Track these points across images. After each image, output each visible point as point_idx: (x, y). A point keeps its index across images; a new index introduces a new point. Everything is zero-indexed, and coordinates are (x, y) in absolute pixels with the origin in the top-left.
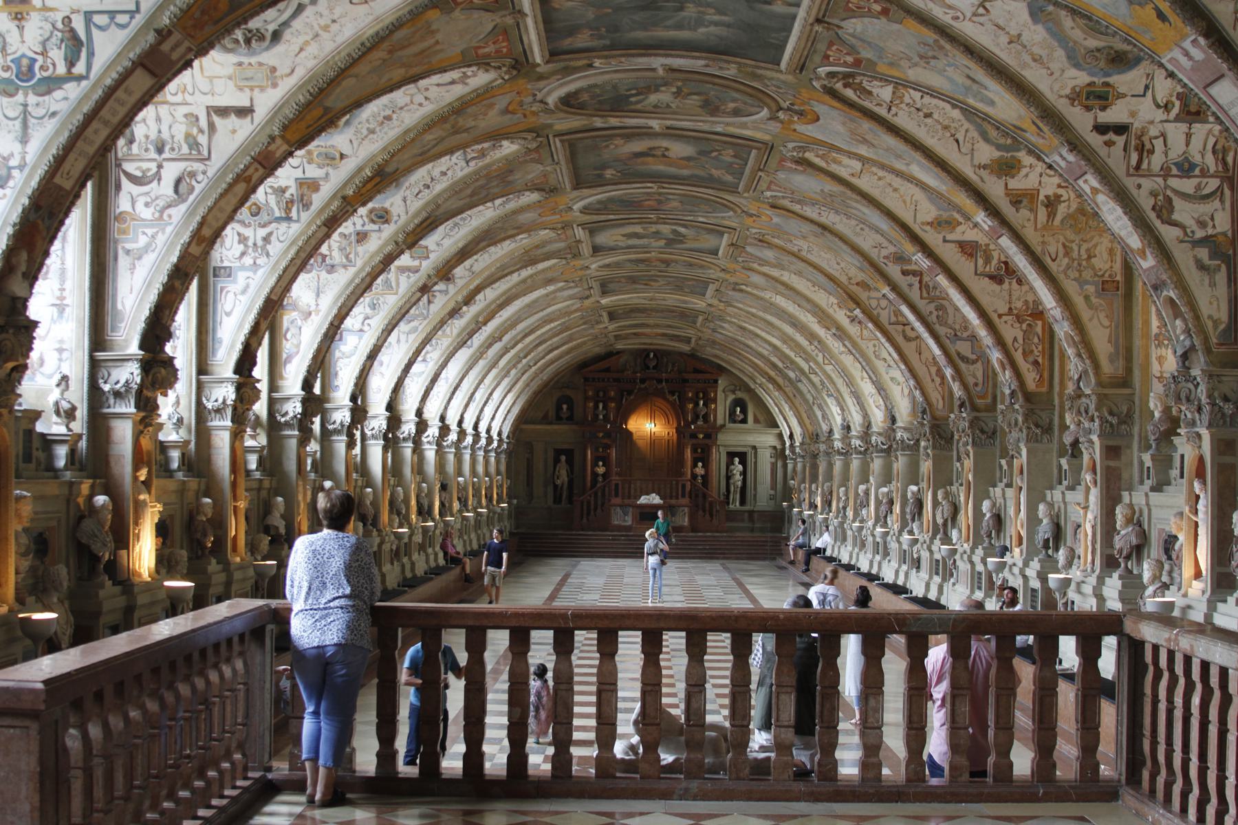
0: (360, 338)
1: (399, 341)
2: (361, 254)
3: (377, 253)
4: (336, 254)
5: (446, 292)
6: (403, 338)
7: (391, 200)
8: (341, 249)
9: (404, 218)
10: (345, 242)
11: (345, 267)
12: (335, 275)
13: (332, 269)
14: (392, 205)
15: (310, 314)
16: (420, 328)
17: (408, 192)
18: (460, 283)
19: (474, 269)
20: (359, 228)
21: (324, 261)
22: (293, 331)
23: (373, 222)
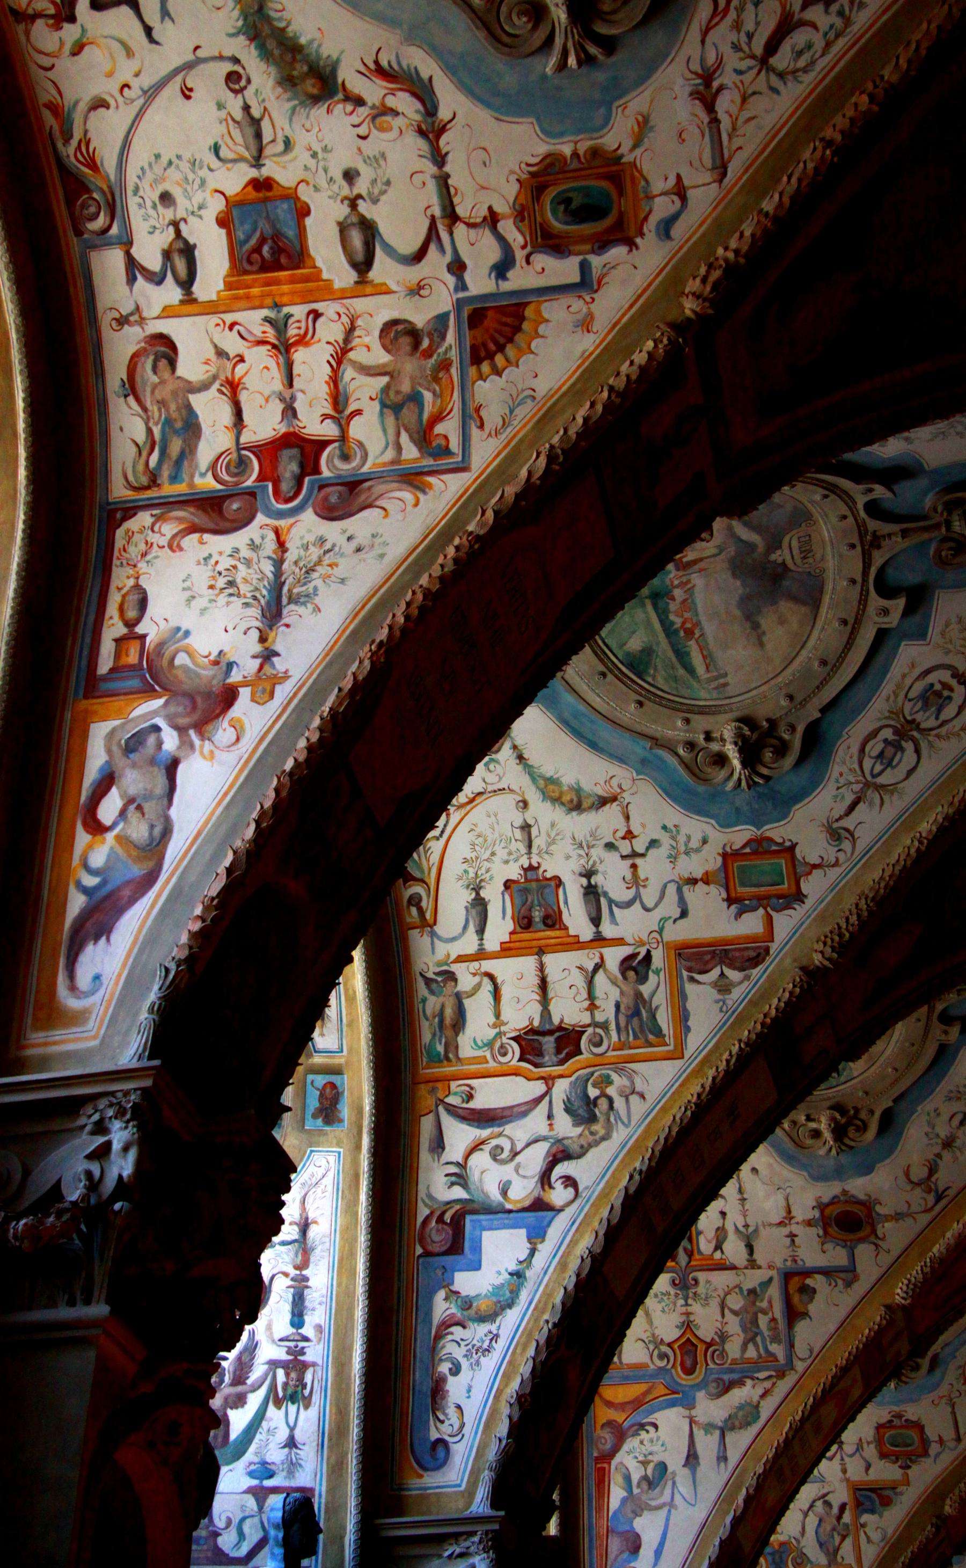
0: (536, 1236)
1: (692, 1459)
2: (492, 416)
3: (575, 392)
4: (369, 430)
5: (849, 1274)
6: (707, 1445)
7: (638, 102)
8: (394, 405)
9: (704, 197)
10: (410, 366)
11: (413, 479)
12: (362, 524)
13: (347, 498)
14: (644, 125)
15: (229, 696)
16: (765, 1414)
17: (723, 34)
18: (895, 1236)
19: (942, 1178)
20: (480, 283)
21: (309, 465)
22: (133, 780)
23: (552, 243)
